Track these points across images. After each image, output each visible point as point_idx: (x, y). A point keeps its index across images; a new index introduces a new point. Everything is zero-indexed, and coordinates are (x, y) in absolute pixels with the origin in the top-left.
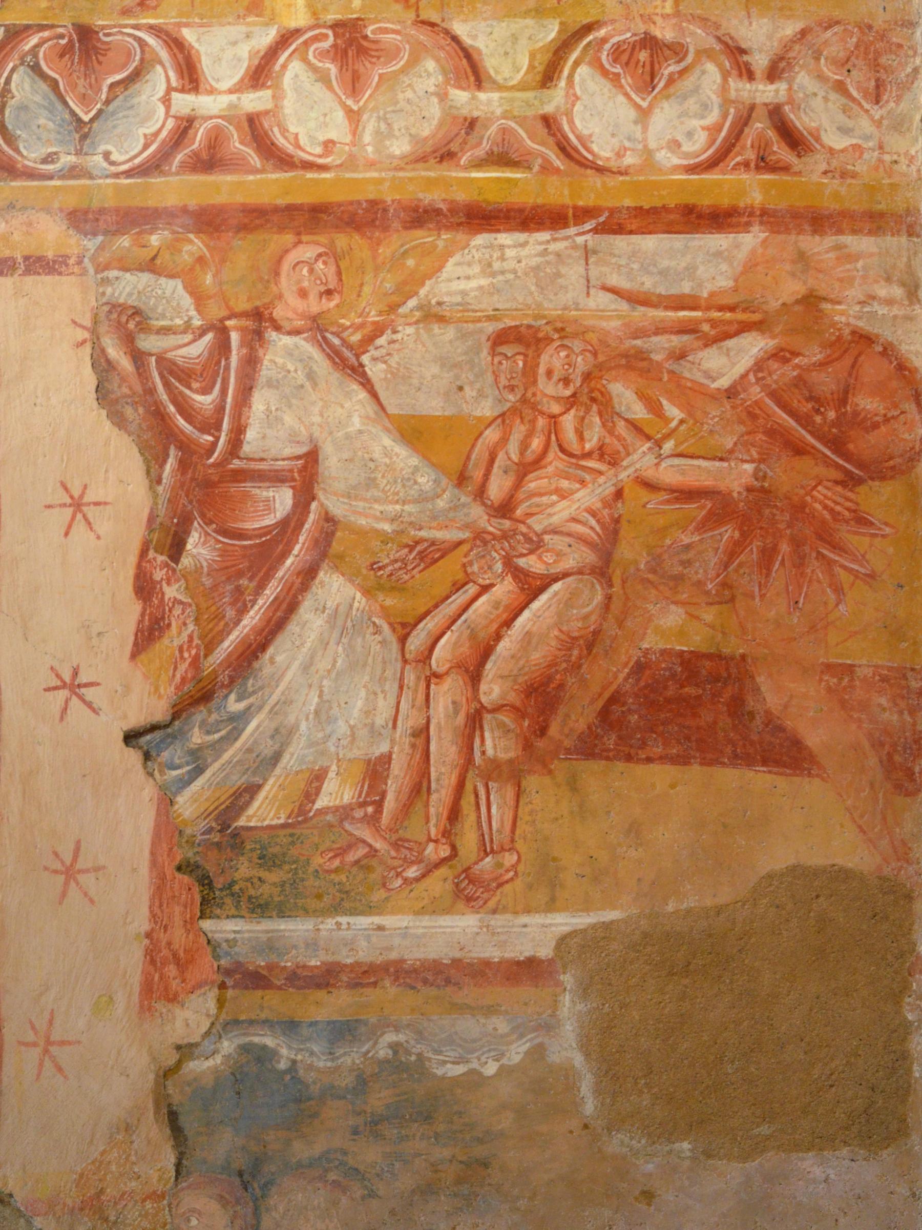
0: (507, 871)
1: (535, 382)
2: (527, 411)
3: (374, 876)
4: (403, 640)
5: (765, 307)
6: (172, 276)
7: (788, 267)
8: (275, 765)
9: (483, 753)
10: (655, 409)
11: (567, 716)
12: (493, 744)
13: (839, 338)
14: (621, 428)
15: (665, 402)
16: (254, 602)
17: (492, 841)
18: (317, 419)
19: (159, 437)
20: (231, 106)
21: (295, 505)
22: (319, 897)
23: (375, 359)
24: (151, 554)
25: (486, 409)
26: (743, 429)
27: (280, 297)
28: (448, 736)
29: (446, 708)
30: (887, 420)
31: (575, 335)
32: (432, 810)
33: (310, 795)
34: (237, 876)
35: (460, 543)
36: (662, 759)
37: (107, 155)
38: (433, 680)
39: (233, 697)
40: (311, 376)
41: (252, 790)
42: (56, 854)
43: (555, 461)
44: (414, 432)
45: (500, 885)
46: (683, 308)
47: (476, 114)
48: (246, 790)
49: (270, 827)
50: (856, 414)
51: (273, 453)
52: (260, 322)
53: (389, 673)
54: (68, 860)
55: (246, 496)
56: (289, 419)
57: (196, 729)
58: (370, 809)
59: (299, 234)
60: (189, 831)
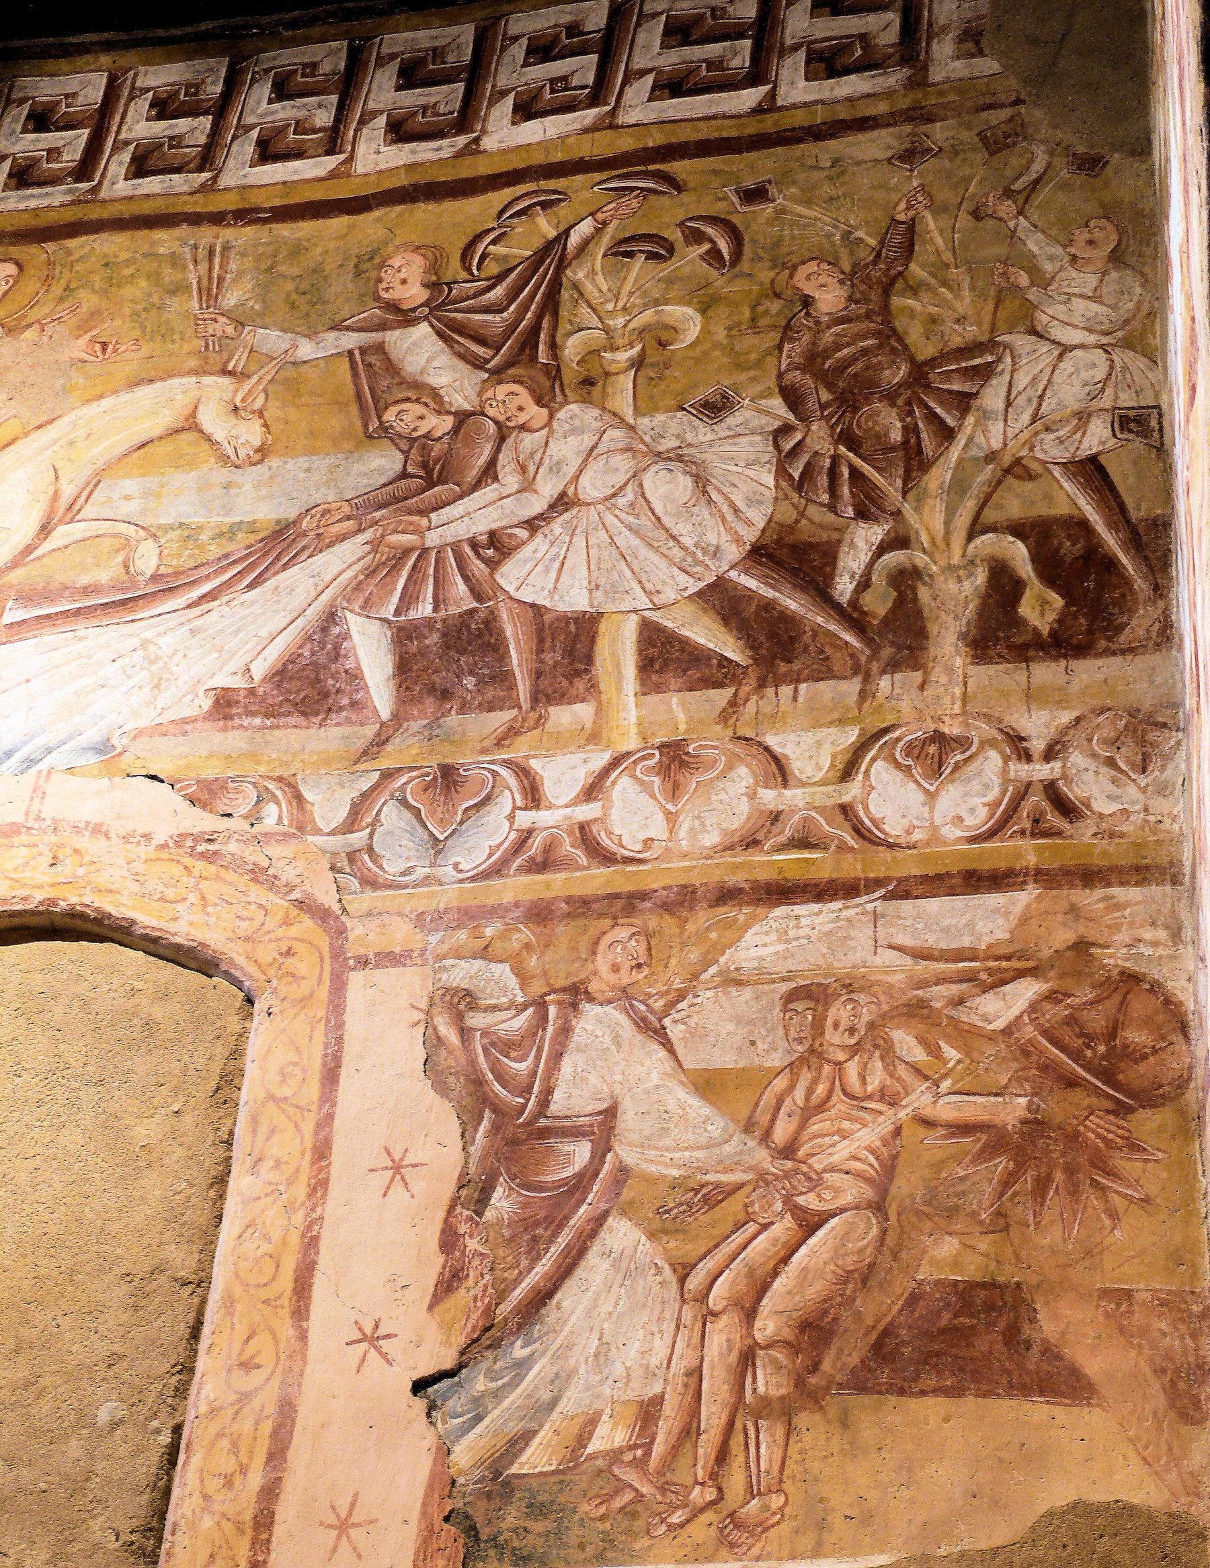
0: (774, 1514)
1: (822, 1033)
2: (814, 1060)
3: (639, 1524)
4: (682, 1280)
5: (1039, 955)
6: (501, 962)
7: (1060, 918)
8: (552, 1410)
9: (755, 1390)
10: (934, 1051)
11: (841, 1350)
12: (766, 1381)
13: (1109, 978)
14: (902, 1071)
15: (943, 1045)
16: (547, 1250)
17: (759, 1482)
18: (619, 1078)
19: (475, 1101)
20: (566, 818)
21: (592, 1157)
22: (582, 1546)
23: (676, 1021)
24: (459, 1209)
25: (776, 1060)
26: (1016, 1065)
27: (595, 973)
28: (721, 1373)
29: (720, 1345)
30: (1155, 1051)
31: (862, 989)
32: (701, 1451)
33: (583, 1439)
34: (504, 1526)
35: (742, 1185)
36: (937, 1391)
37: (456, 865)
38: (710, 1318)
39: (519, 1343)
40: (616, 1039)
41: (527, 1436)
42: (333, 1508)
43: (839, 1104)
44: (708, 1085)
45: (766, 1530)
46: (962, 960)
47: (781, 808)
48: (522, 1437)
49: (541, 1474)
50: (1125, 1046)
51: (577, 1110)
52: (576, 995)
53: (667, 1314)
54: (343, 1515)
55: (550, 1150)
56: (593, 1079)
57: (481, 1377)
58: (639, 1452)
59: (615, 918)
60: (461, 1480)
